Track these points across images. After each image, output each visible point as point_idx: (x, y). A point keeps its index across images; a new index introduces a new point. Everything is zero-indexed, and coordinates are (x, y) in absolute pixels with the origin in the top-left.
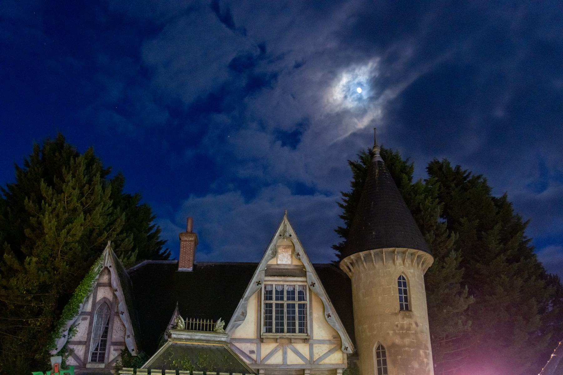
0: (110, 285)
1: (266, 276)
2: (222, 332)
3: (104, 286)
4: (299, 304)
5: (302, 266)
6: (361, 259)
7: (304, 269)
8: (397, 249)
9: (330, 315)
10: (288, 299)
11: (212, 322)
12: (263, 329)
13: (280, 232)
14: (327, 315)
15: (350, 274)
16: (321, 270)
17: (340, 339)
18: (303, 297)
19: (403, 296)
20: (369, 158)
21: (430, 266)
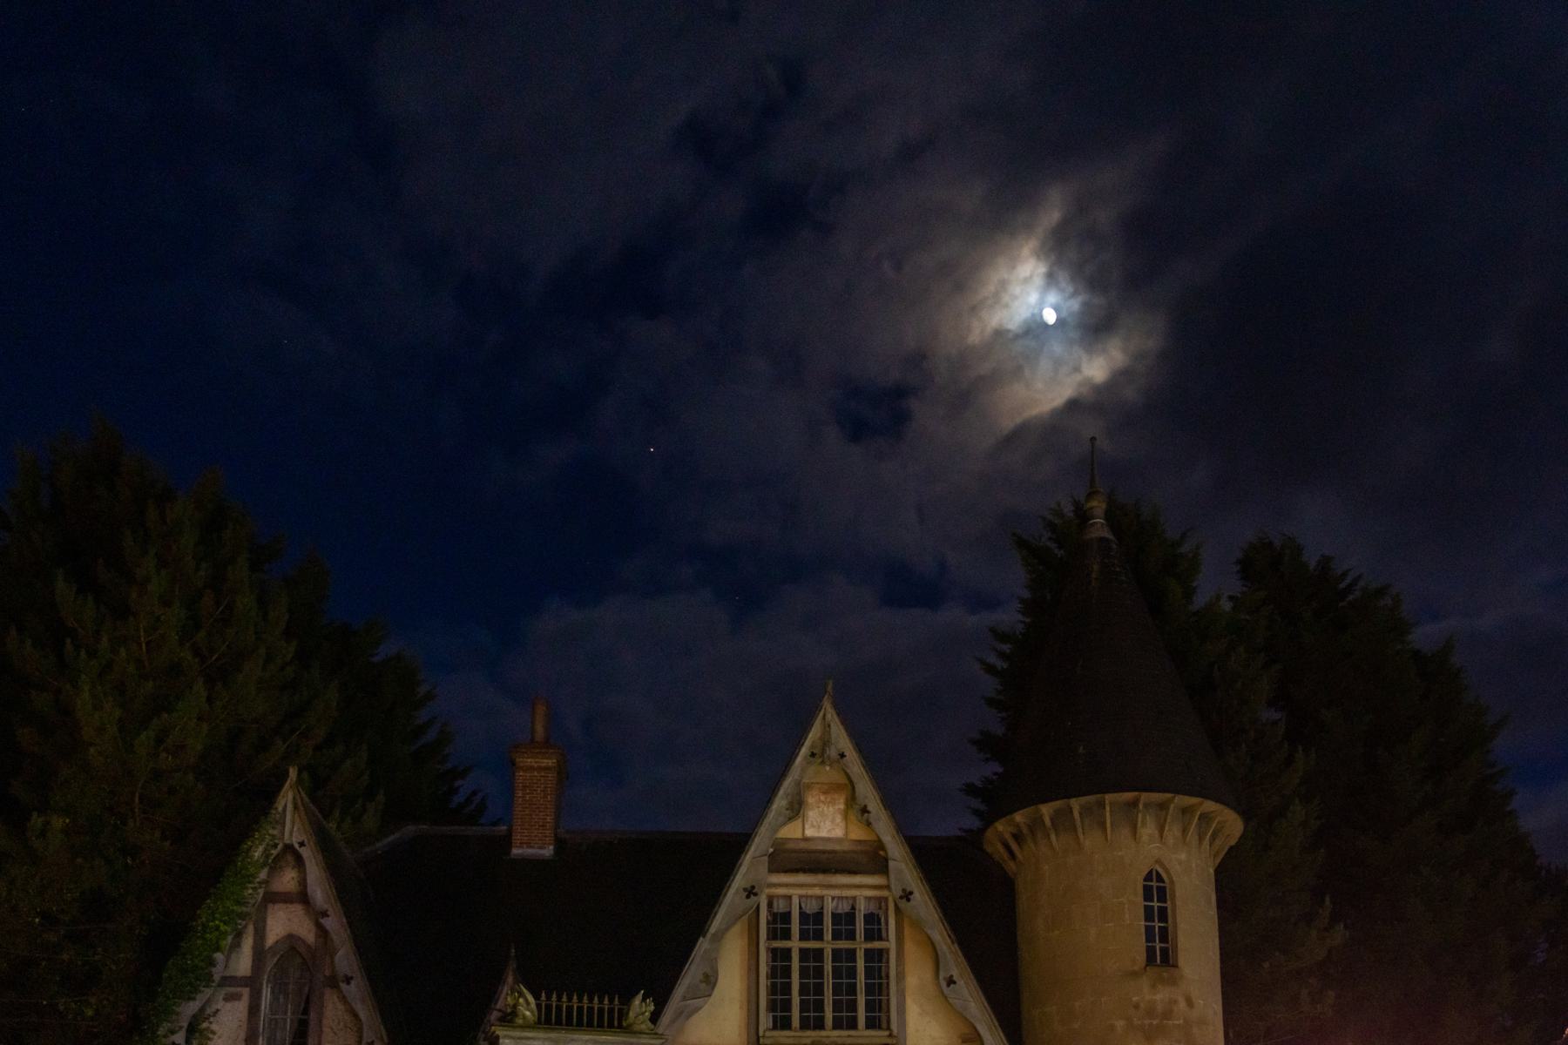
0: (303, 897)
1: (772, 870)
2: (647, 1031)
3: (285, 902)
4: (866, 950)
6: (1043, 821)
7: (881, 853)
8: (1145, 797)
9: (955, 978)
10: (837, 936)
11: (616, 1002)
12: (765, 1020)
13: (812, 746)
14: (945, 979)
15: (1011, 866)
16: (925, 853)
21: (1233, 842)
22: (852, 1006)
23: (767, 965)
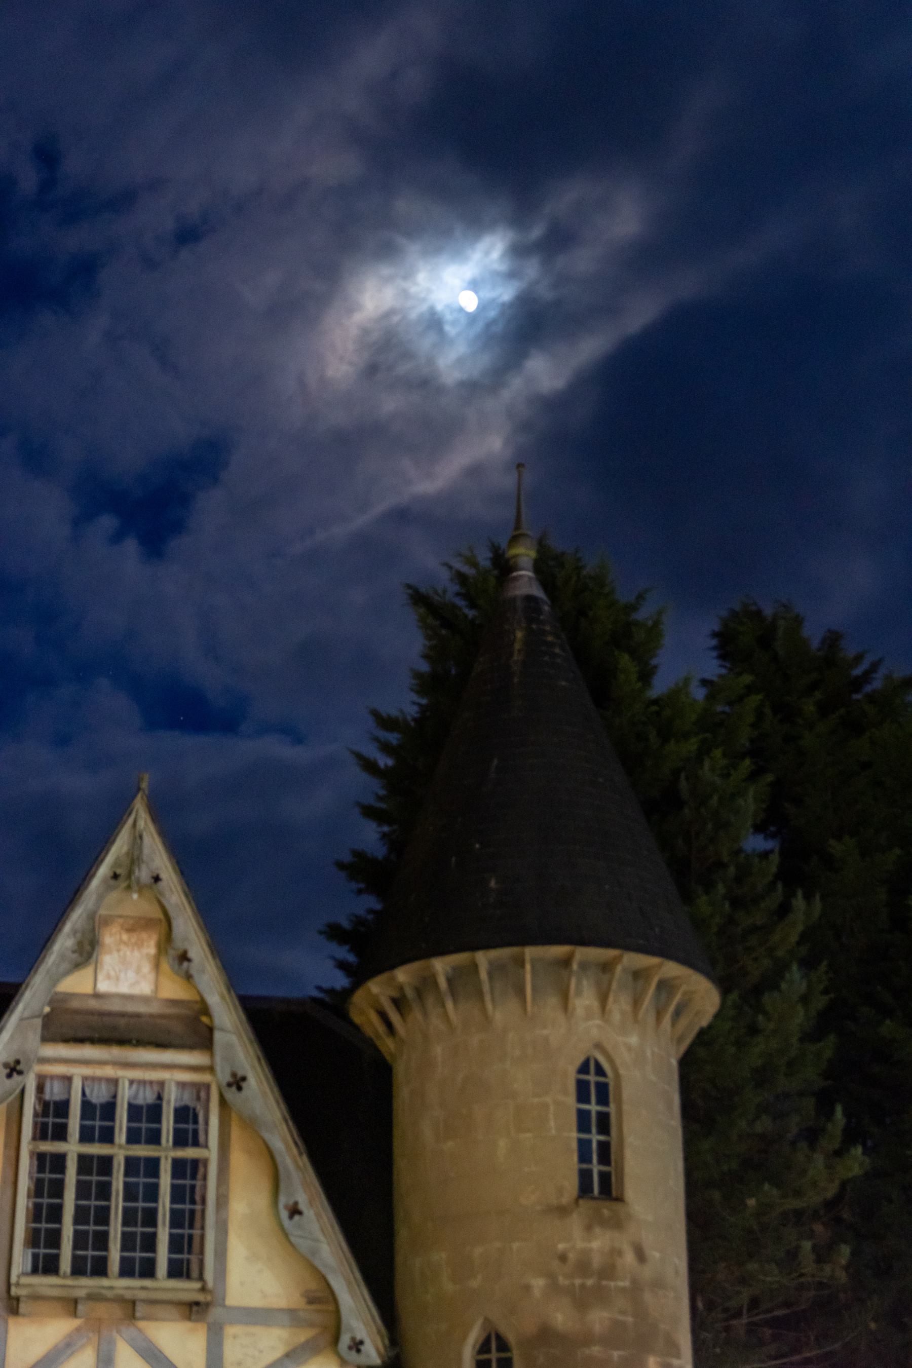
1: (48, 1038)
5: (197, 1007)
7: (204, 1019)
8: (583, 953)
9: (302, 1206)
10: (133, 1137)
13: (117, 863)
14: (286, 1207)
15: (388, 1045)
17: (331, 1308)
18: (196, 1132)
19: (595, 1138)
20: (492, 581)
21: (705, 1022)
22: (150, 1243)
23: (31, 1178)
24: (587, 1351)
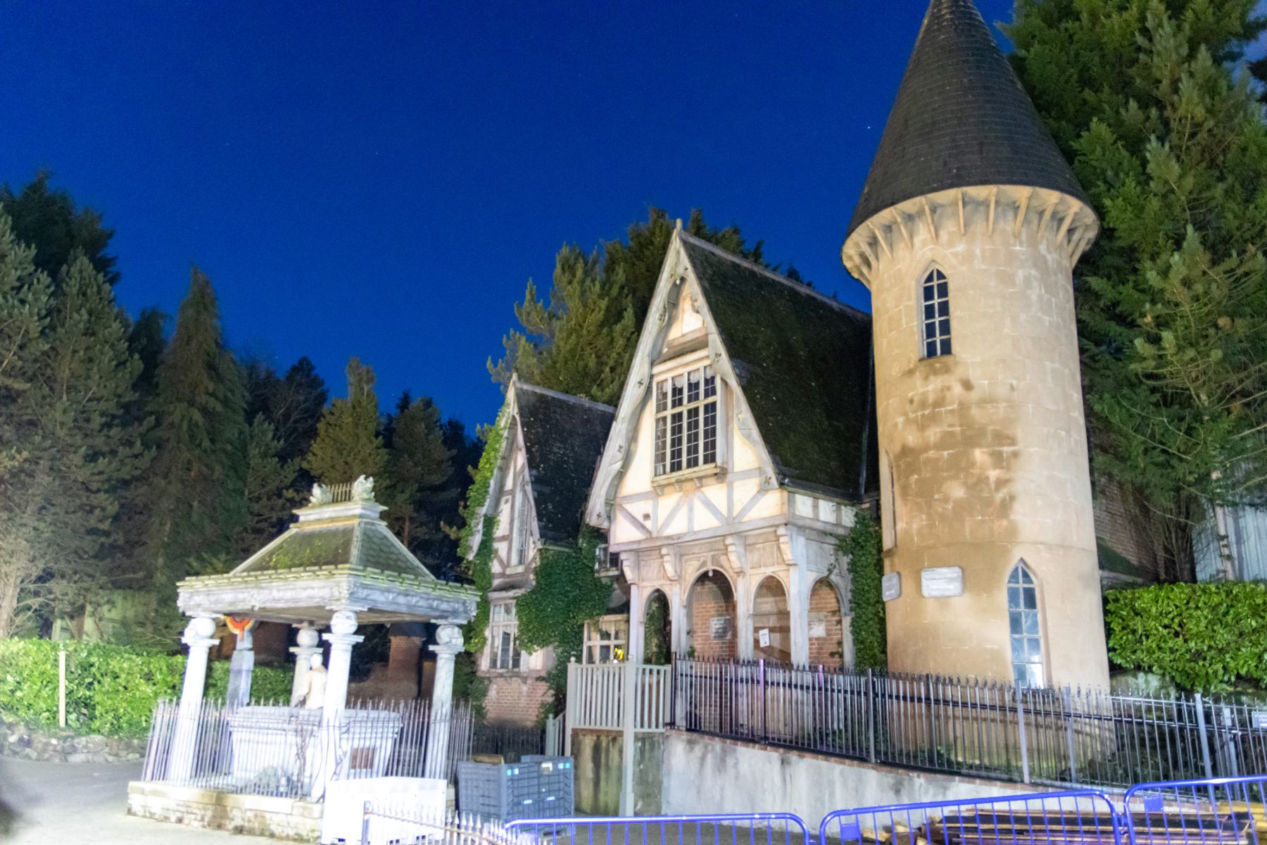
24: (925, 455)
